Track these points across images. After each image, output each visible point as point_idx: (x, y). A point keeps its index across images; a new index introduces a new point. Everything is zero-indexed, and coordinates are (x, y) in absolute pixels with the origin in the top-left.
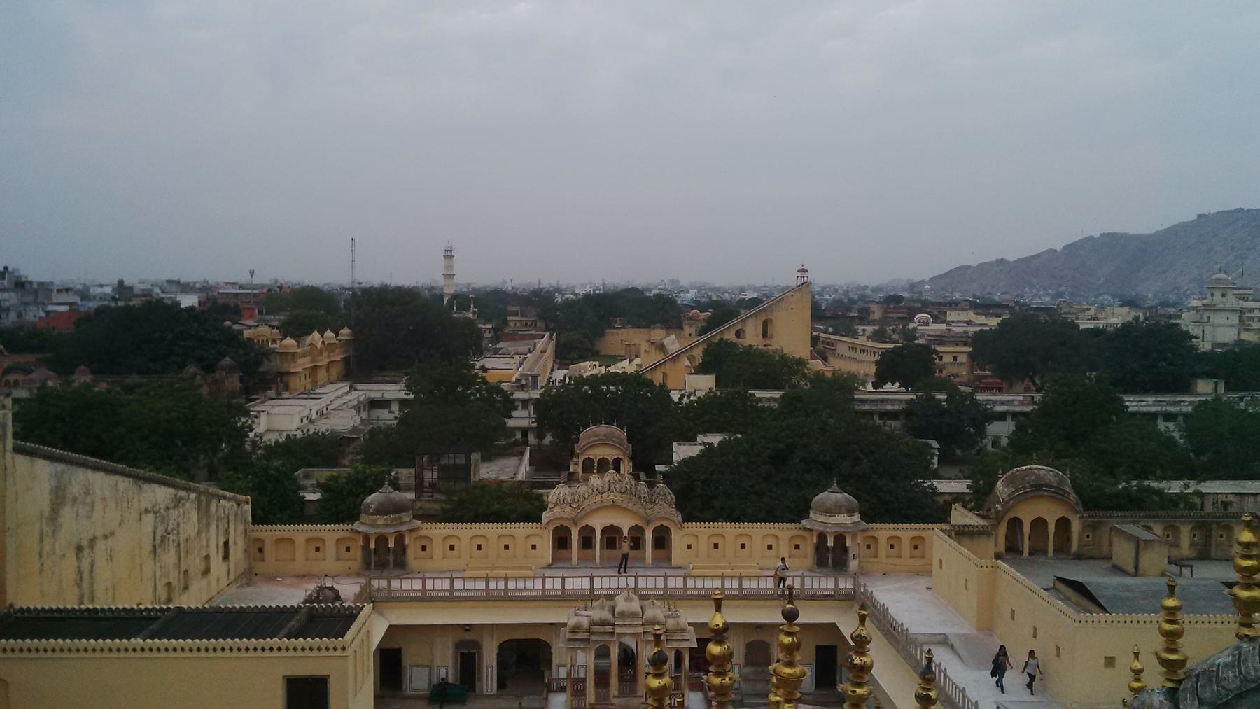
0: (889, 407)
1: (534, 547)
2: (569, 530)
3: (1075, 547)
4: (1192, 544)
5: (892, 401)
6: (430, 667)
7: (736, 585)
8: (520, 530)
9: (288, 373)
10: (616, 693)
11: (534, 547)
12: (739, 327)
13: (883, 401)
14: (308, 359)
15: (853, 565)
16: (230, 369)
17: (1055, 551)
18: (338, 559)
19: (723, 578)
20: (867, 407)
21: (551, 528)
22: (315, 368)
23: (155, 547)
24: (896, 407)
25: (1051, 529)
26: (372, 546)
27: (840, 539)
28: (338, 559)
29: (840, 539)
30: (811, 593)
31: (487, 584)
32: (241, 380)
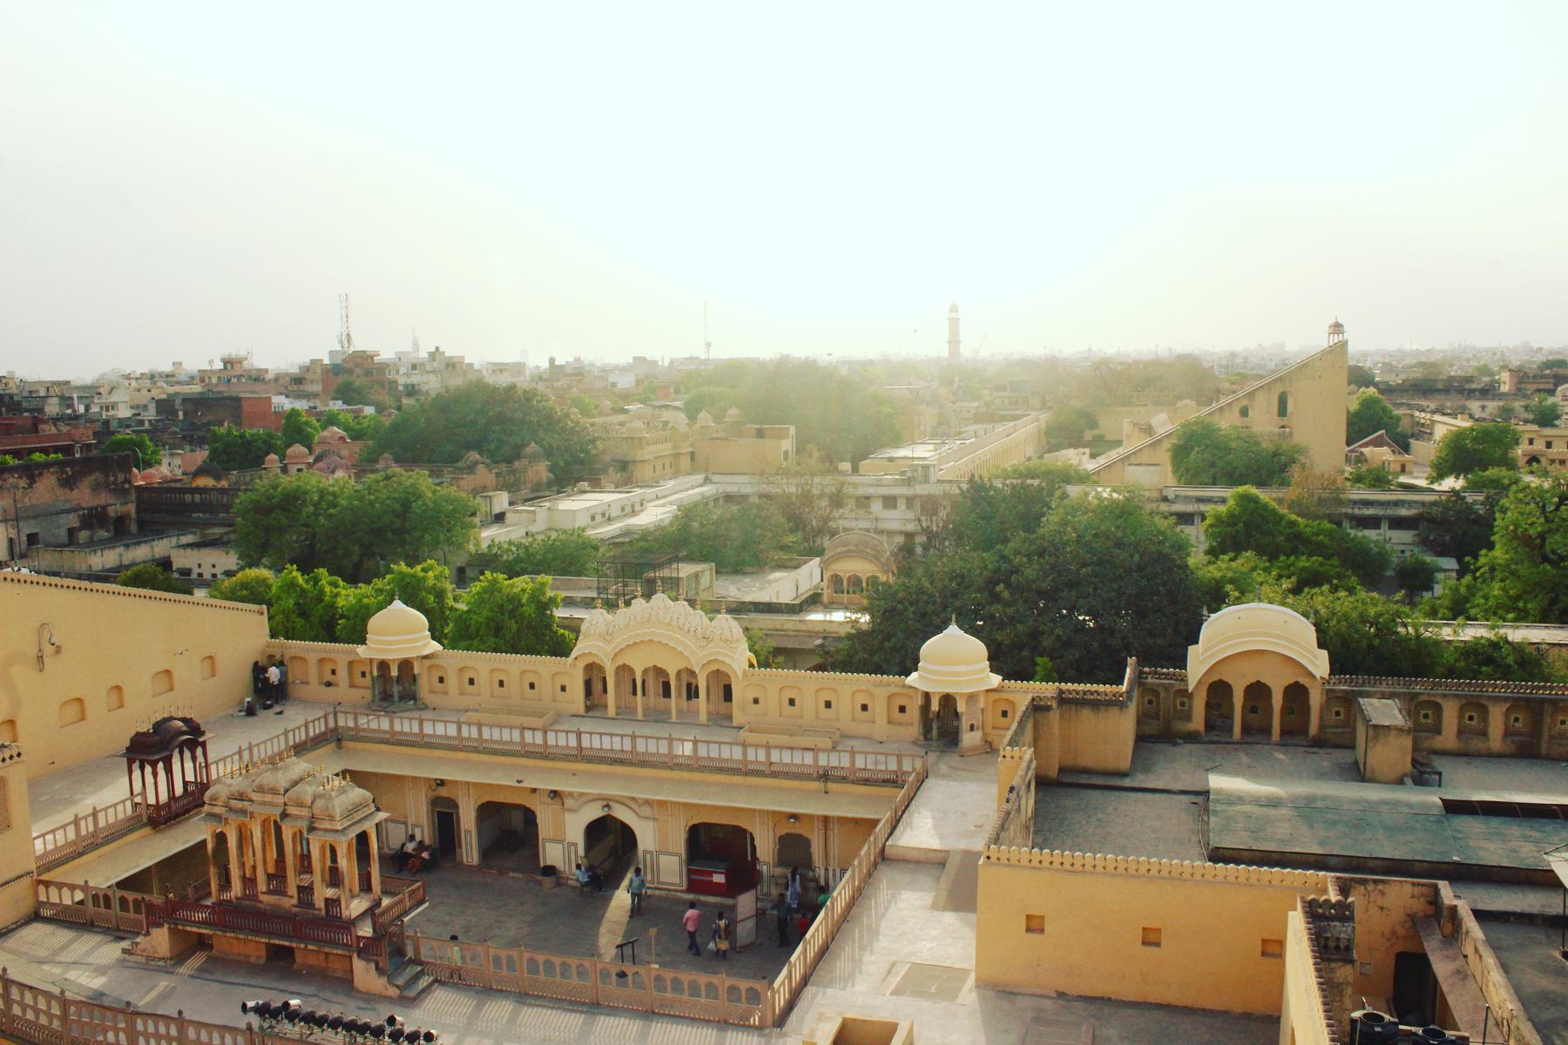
0: (1404, 512)
1: (563, 689)
2: (601, 669)
3: (1313, 729)
4: (1508, 733)
5: (1410, 504)
6: (405, 823)
7: (762, 757)
8: (543, 666)
9: (634, 462)
11: (563, 689)
12: (1245, 402)
13: (1397, 504)
14: (669, 445)
15: (969, 739)
16: (534, 458)
17: (1285, 732)
19: (768, 747)
20: (1370, 512)
21: (581, 664)
22: (676, 455)
24: (1413, 512)
25: (1277, 701)
28: (352, 686)
30: (865, 775)
31: (459, 729)
32: (551, 470)
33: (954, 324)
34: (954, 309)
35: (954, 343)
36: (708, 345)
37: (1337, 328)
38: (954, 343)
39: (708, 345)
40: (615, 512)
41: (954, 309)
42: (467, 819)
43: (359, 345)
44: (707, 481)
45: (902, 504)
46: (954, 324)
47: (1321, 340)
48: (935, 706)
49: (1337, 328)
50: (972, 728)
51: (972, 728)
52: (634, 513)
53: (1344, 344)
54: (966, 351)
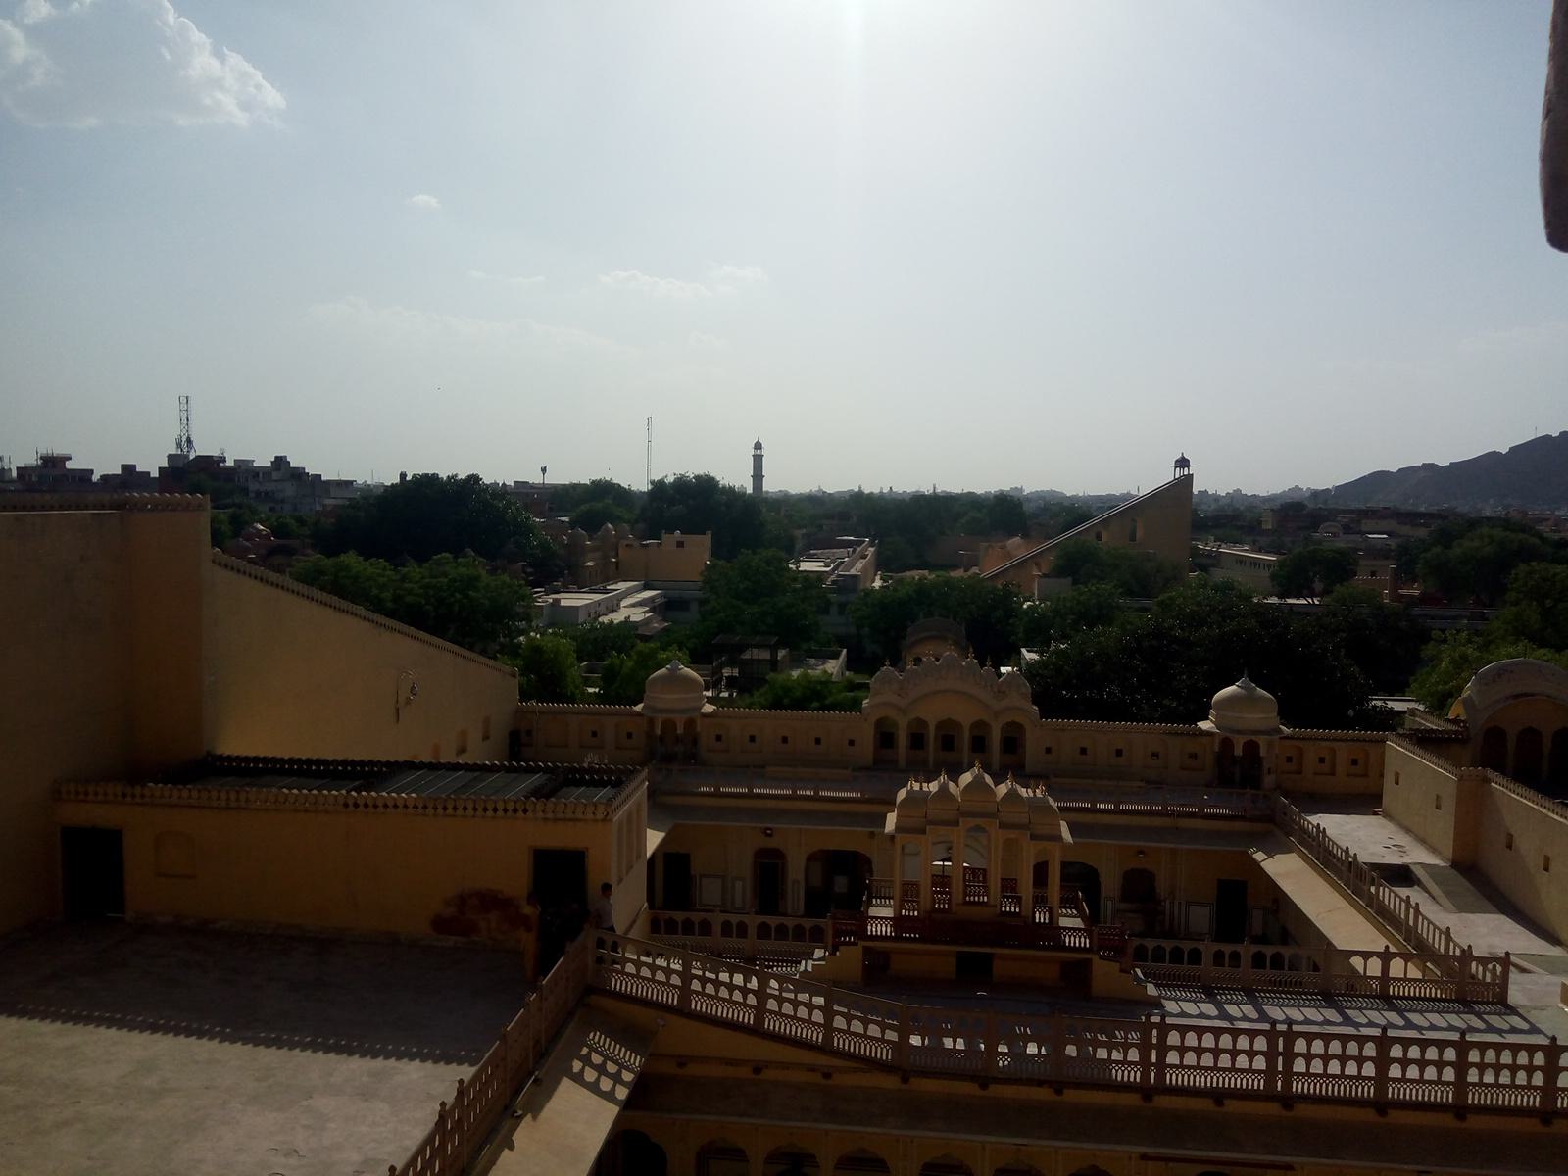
10: (961, 900)
18: (618, 748)
23: (398, 709)
26: (658, 732)
27: (1251, 747)
28: (618, 748)
29: (1251, 747)
33: (758, 460)
34: (758, 446)
35: (758, 477)
36: (544, 470)
37: (1183, 462)
38: (758, 477)
39: (544, 470)
40: (602, 609)
41: (758, 446)
42: (796, 869)
43: (203, 448)
44: (646, 587)
45: (834, 609)
46: (758, 460)
47: (1164, 475)
48: (1238, 751)
49: (1183, 462)
50: (1269, 773)
51: (1269, 773)
52: (612, 611)
53: (1190, 477)
54: (771, 486)
